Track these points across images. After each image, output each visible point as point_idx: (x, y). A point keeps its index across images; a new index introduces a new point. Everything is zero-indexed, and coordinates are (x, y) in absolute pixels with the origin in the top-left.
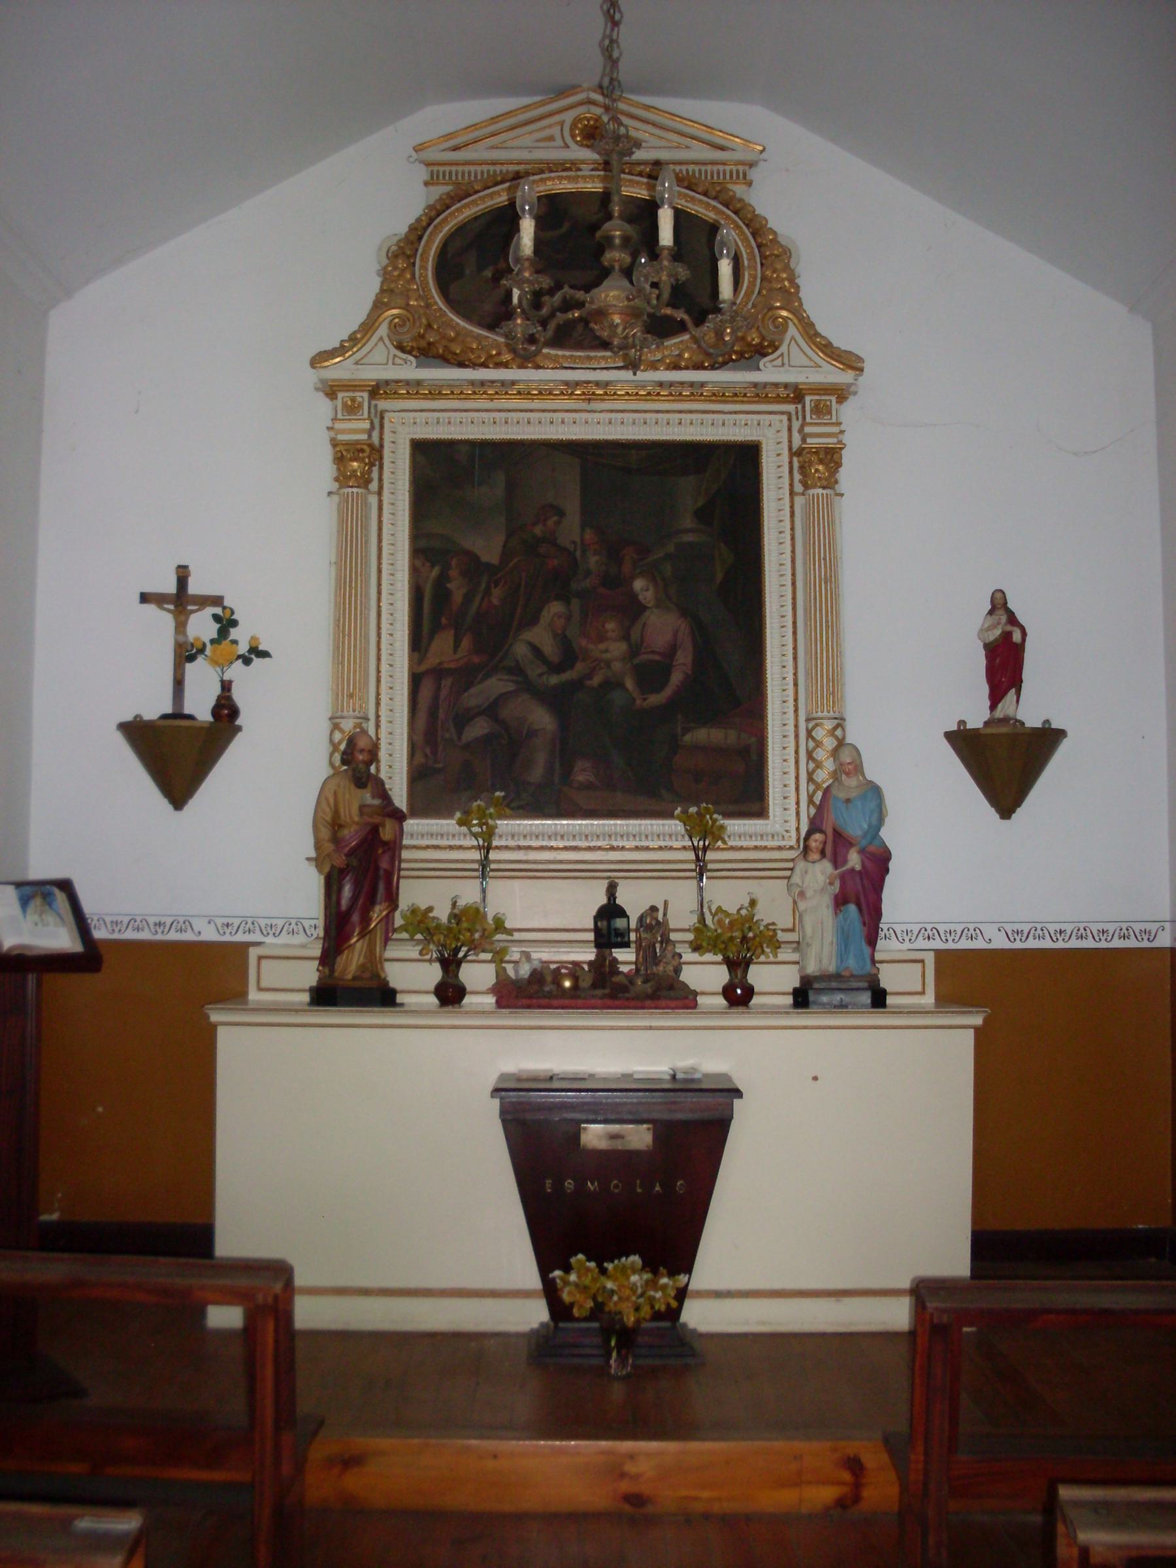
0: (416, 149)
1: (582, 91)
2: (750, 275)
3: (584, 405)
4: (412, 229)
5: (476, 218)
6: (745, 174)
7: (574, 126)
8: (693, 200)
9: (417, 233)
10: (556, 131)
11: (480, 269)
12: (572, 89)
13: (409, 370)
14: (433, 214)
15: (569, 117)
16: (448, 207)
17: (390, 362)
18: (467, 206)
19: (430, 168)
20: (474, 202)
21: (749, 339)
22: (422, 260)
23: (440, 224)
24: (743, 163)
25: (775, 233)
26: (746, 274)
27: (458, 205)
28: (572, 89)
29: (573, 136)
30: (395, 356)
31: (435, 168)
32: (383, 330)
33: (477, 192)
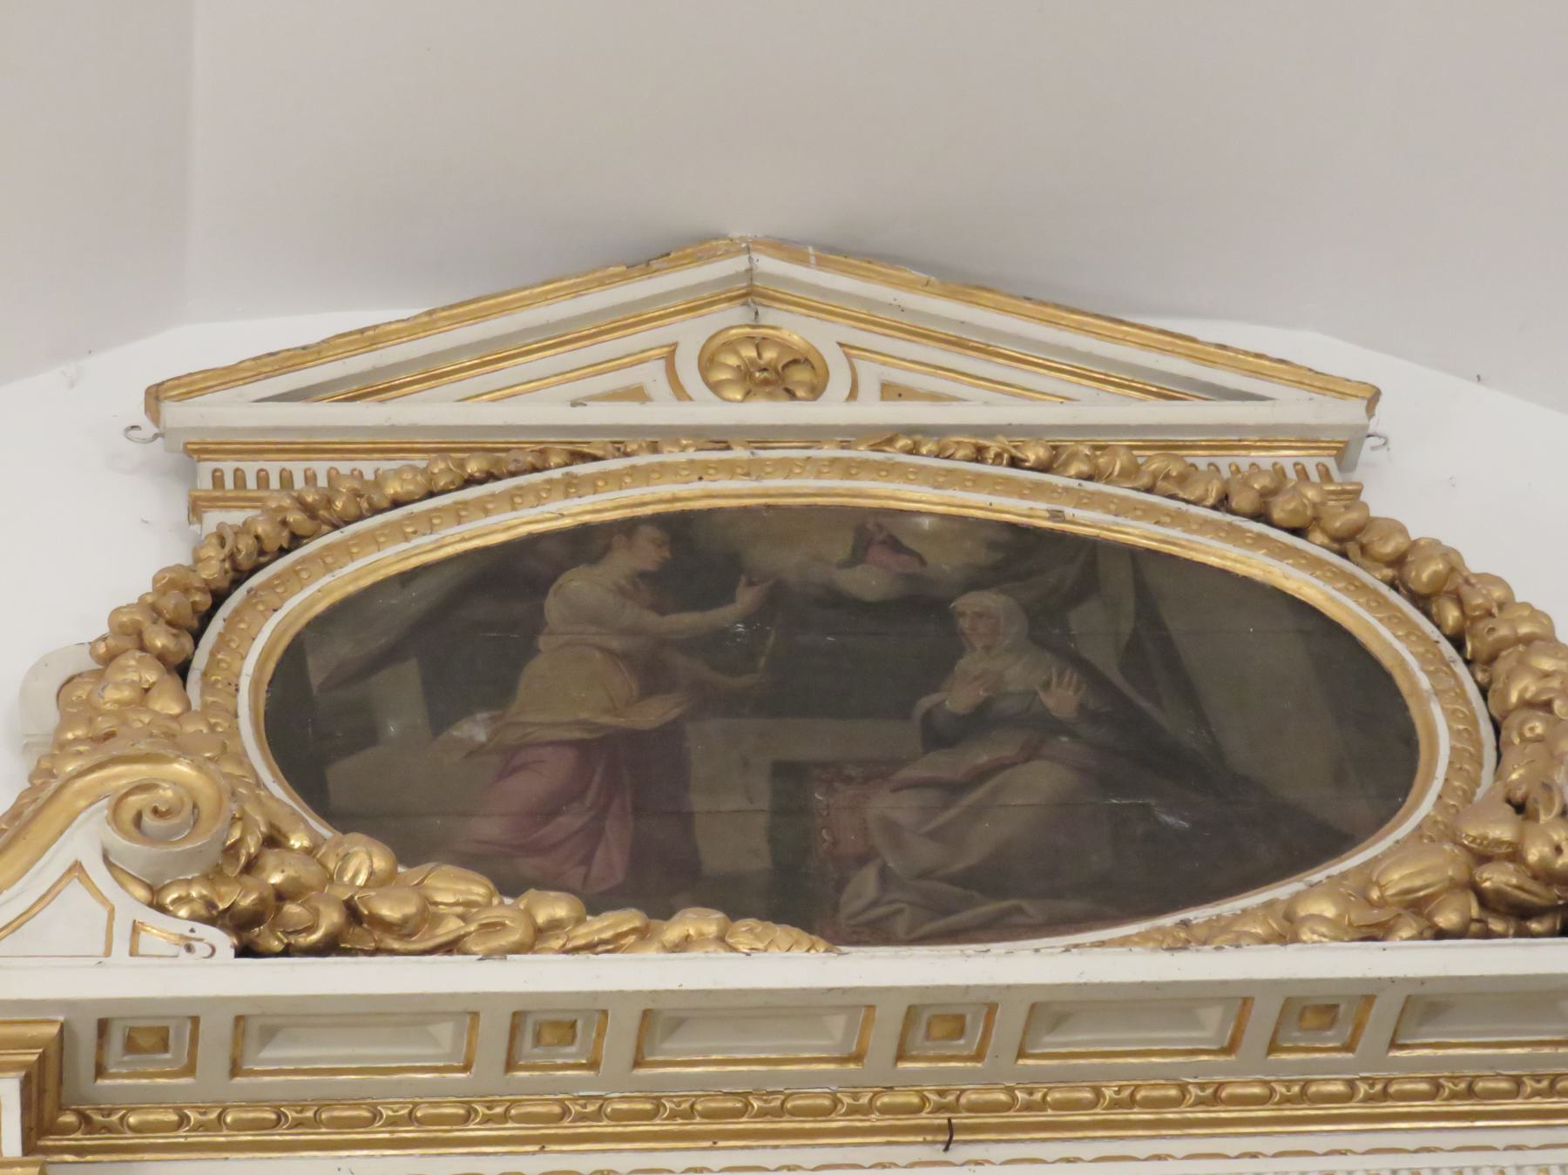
0: (155, 396)
1: (728, 254)
2: (1451, 715)
3: (936, 1153)
4: (170, 582)
5: (406, 578)
6: (1326, 475)
7: (707, 362)
8: (1178, 519)
9: (188, 615)
10: (651, 375)
11: (440, 722)
12: (698, 246)
13: (218, 975)
14: (246, 545)
15: (691, 334)
16: (296, 540)
17: (121, 946)
18: (371, 540)
19: (206, 468)
20: (398, 532)
21: (1533, 855)
22: (207, 685)
23: (268, 586)
24: (1307, 438)
25: (1498, 581)
26: (1436, 711)
27: (335, 536)
28: (700, 246)
29: (715, 387)
30: (136, 929)
31: (228, 466)
32: (85, 838)
33: (396, 504)
